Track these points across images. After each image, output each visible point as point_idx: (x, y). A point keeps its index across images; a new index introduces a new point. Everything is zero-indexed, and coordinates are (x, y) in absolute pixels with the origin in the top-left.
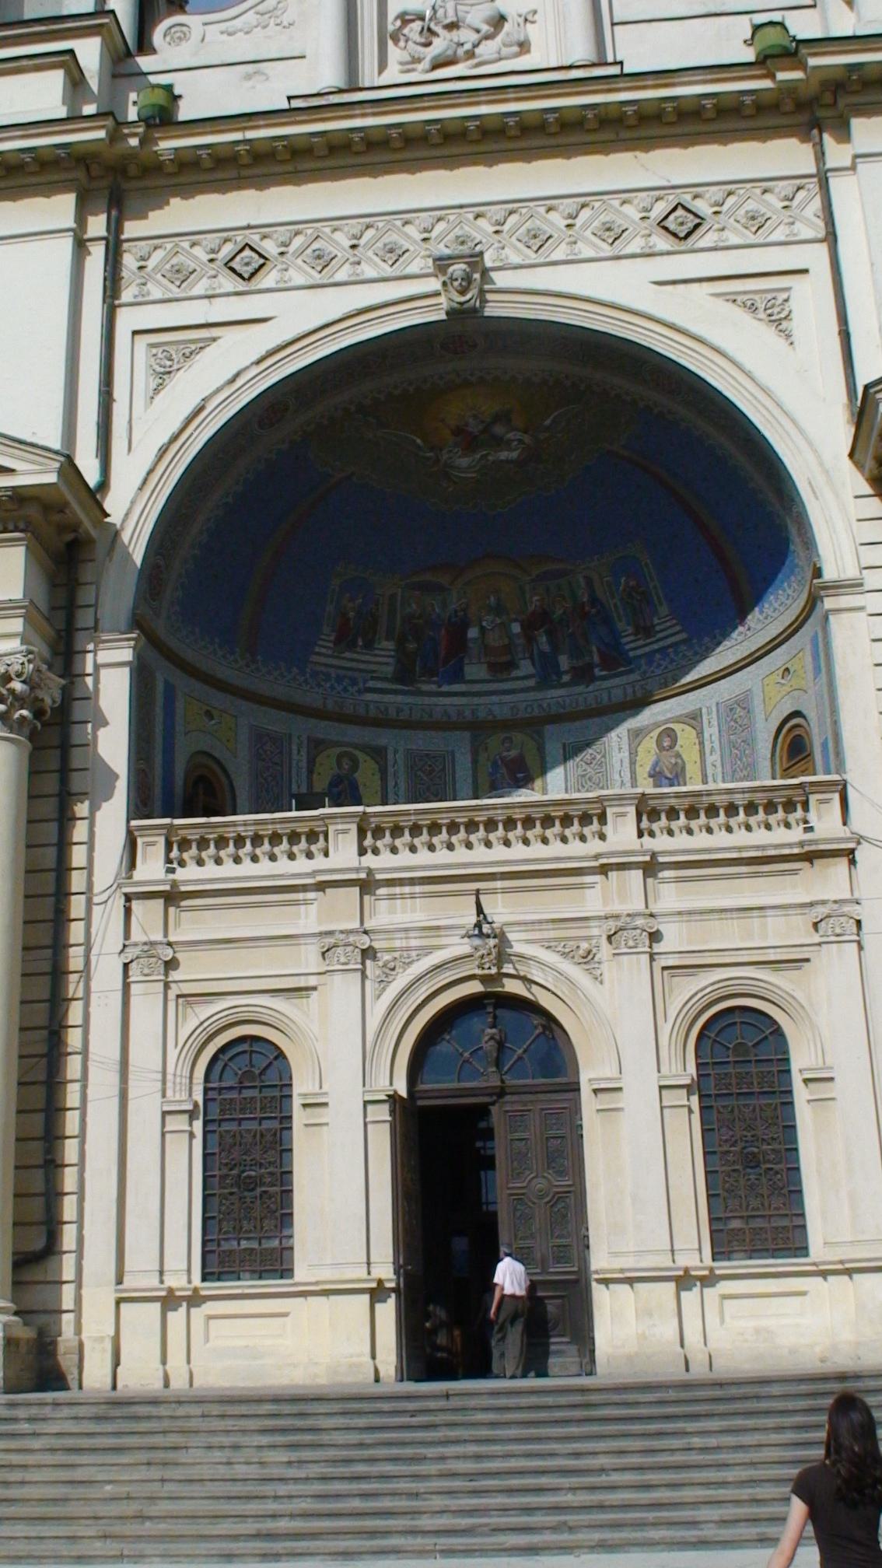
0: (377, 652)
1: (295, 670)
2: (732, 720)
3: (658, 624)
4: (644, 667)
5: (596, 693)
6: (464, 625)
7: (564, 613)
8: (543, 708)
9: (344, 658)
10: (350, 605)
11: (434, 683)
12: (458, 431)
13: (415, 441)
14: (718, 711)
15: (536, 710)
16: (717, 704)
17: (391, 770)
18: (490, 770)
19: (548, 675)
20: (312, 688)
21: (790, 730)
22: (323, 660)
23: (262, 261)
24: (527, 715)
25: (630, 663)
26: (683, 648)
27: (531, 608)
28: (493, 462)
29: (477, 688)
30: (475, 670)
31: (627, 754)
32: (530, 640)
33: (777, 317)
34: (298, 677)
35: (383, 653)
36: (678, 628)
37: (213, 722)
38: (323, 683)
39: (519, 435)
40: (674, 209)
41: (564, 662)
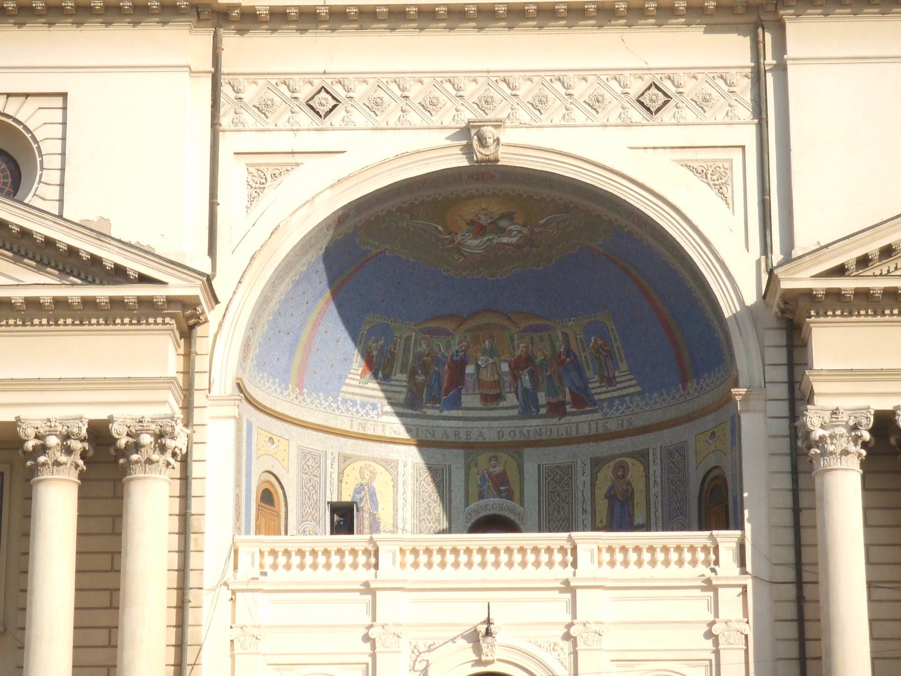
0: (392, 382)
1: (331, 399)
2: (672, 462)
3: (619, 377)
4: (605, 410)
5: (567, 425)
6: (462, 364)
7: (545, 359)
8: (523, 433)
9: (367, 388)
10: (375, 345)
11: (437, 408)
12: (472, 223)
13: (437, 228)
14: (661, 453)
15: (518, 435)
16: (661, 447)
17: (400, 480)
18: (479, 482)
19: (528, 408)
20: (342, 412)
21: (712, 480)
22: (351, 390)
23: (335, 103)
24: (510, 439)
25: (595, 404)
26: (637, 398)
27: (518, 353)
28: (496, 244)
29: (470, 414)
30: (470, 399)
31: (589, 478)
32: (516, 378)
33: (720, 181)
34: (332, 404)
35: (397, 383)
36: (634, 382)
37: (274, 446)
38: (350, 409)
39: (519, 228)
40: (649, 88)
41: (542, 398)
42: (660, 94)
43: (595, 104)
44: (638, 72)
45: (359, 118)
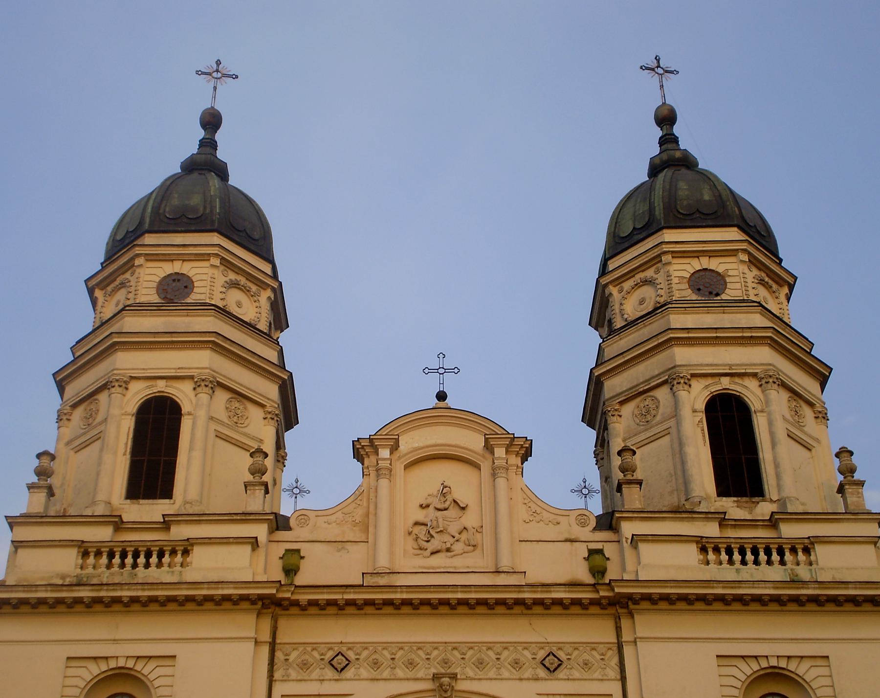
23: (347, 662)
42: (555, 659)
43: (516, 664)
44: (541, 645)
45: (364, 673)
